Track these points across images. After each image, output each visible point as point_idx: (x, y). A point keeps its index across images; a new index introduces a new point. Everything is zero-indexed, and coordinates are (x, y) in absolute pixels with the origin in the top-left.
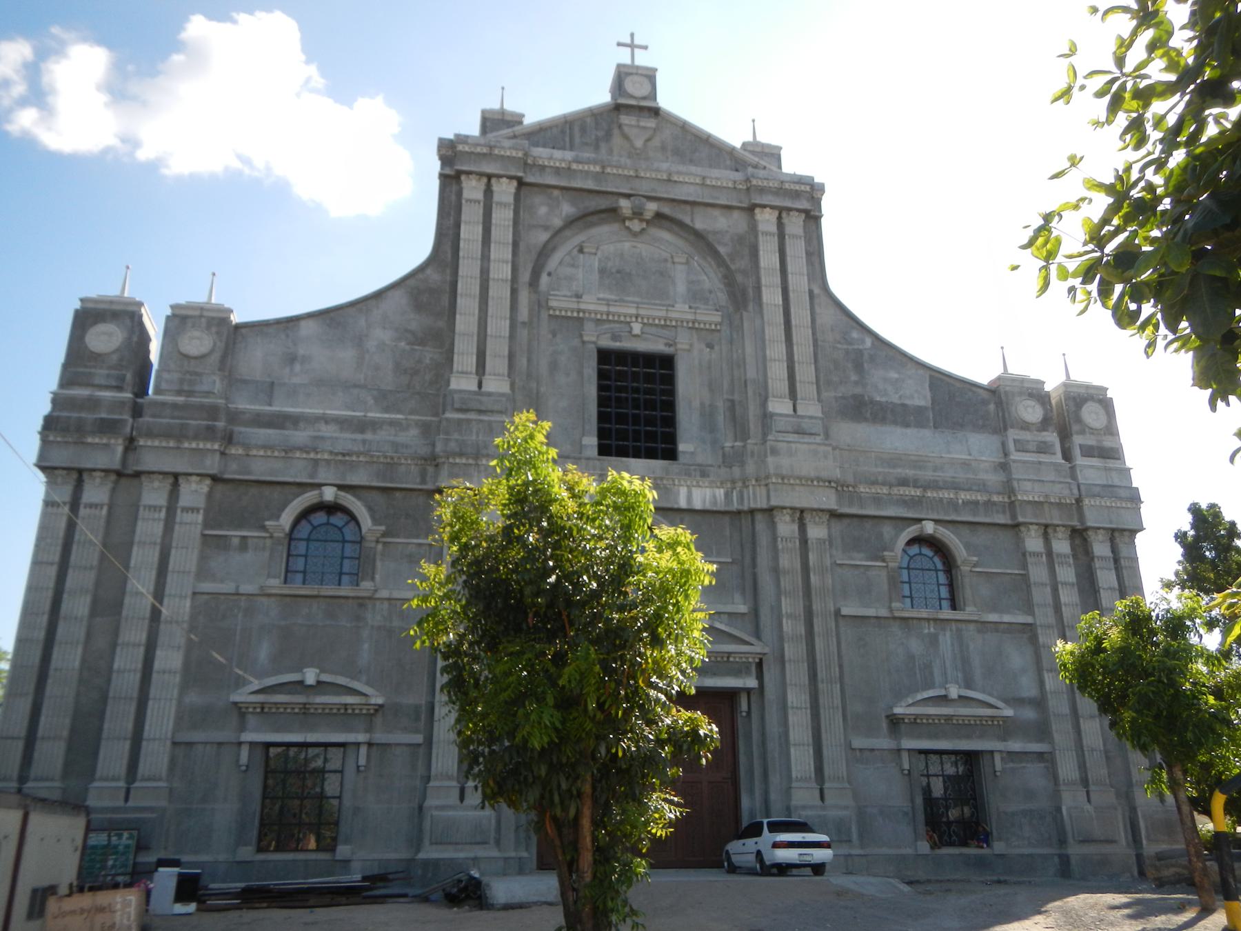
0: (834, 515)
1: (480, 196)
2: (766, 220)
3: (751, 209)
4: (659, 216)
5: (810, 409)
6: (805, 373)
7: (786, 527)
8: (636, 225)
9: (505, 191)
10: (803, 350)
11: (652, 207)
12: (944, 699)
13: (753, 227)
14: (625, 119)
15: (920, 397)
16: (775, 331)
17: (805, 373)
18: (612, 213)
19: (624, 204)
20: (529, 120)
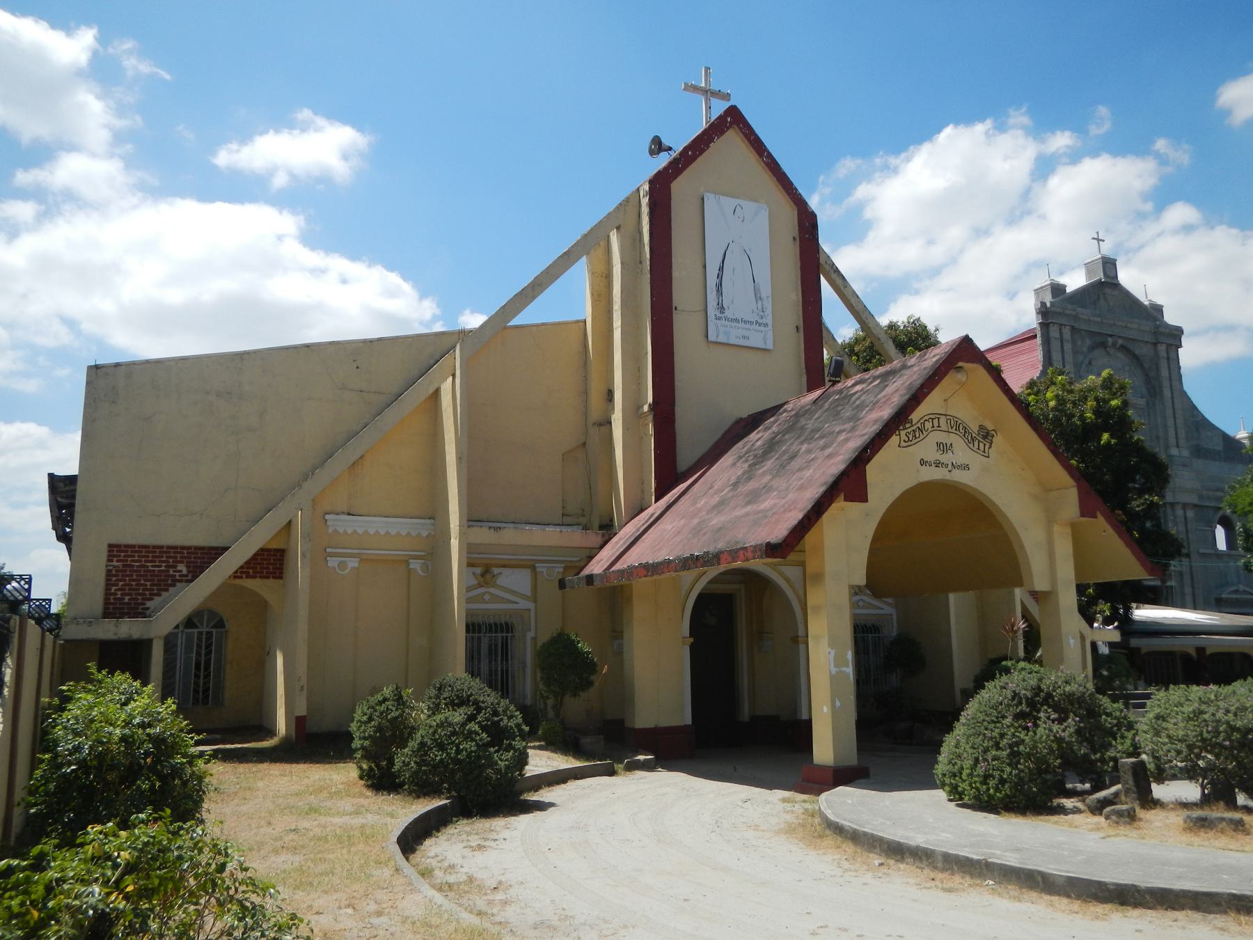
0: (1195, 506)
1: (1058, 336)
2: (1162, 349)
3: (1155, 344)
4: (1122, 346)
5: (1185, 453)
6: (1182, 434)
7: (1180, 512)
8: (1112, 351)
9: (1067, 332)
10: (1180, 421)
11: (1120, 342)
12: (1236, 592)
13: (1156, 351)
14: (1108, 291)
15: (1219, 446)
16: (1169, 412)
17: (1182, 434)
18: (1103, 345)
19: (1110, 340)
20: (1068, 290)
